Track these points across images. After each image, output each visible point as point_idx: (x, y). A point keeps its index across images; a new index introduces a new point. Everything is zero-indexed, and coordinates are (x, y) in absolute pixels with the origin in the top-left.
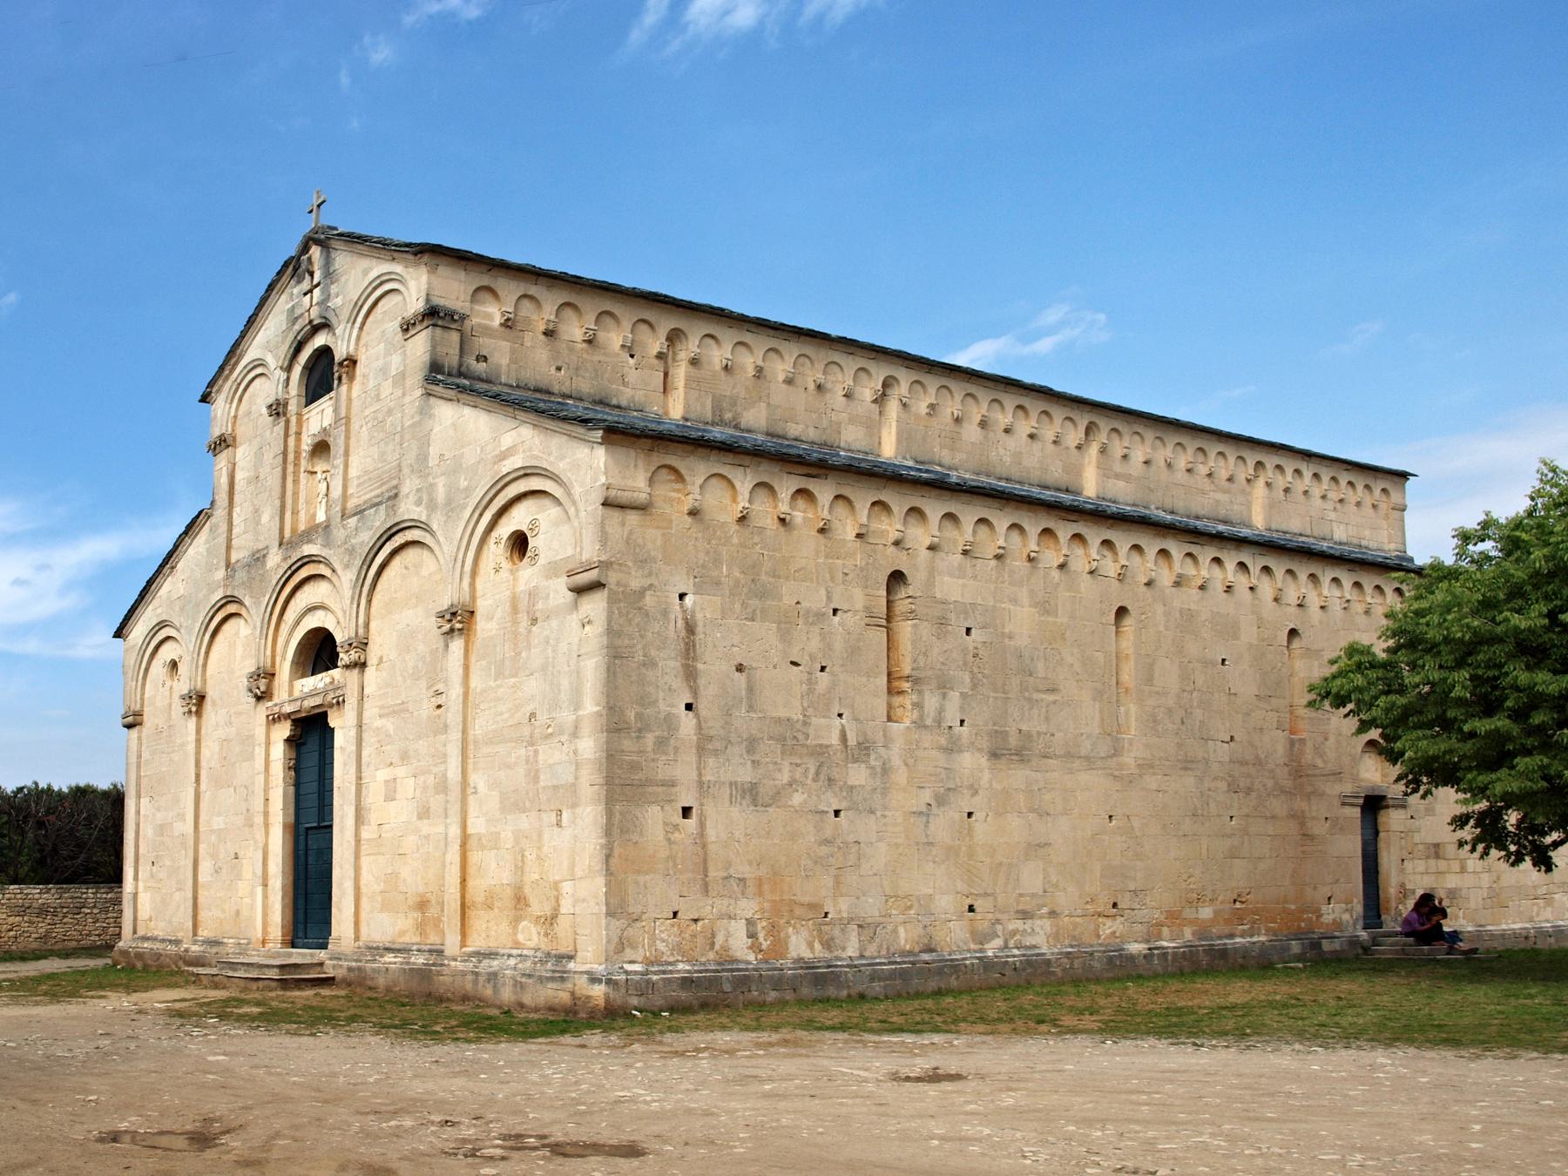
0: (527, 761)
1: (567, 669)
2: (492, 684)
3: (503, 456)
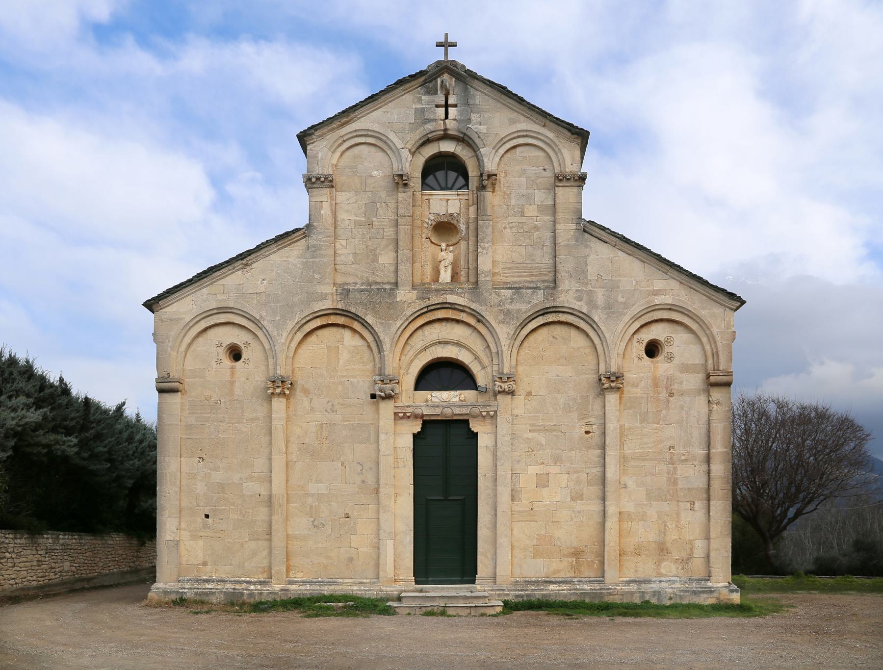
0: (668, 473)
1: (696, 425)
2: (638, 425)
3: (657, 293)
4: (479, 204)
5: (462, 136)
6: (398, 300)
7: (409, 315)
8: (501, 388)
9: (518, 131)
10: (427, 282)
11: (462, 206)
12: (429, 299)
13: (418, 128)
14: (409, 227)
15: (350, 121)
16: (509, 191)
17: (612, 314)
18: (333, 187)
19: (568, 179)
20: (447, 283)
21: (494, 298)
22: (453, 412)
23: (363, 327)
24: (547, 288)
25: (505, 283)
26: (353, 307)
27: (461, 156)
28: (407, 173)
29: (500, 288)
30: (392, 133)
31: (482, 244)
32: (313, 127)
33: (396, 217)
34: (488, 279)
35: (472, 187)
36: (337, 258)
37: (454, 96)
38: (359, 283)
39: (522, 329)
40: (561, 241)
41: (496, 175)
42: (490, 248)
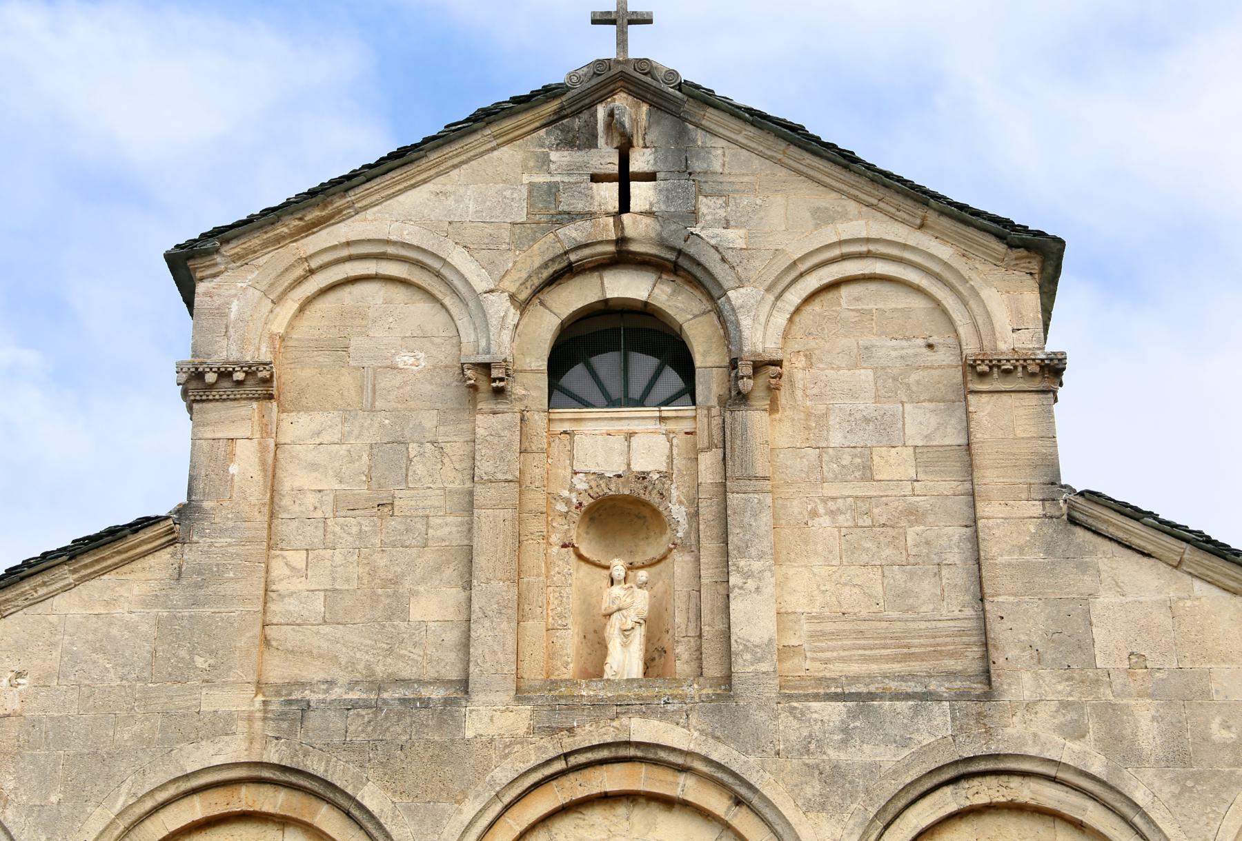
4: (728, 445)
5: (671, 256)
6: (469, 734)
7: (505, 782)
9: (841, 243)
10: (567, 677)
11: (675, 452)
12: (571, 730)
13: (538, 235)
14: (508, 514)
15: (331, 217)
16: (821, 408)
17: (1197, 782)
18: (270, 397)
19: (1007, 372)
20: (630, 681)
21: (788, 729)
23: (348, 822)
24: (962, 695)
25: (820, 681)
26: (316, 758)
27: (670, 313)
28: (505, 361)
29: (807, 697)
30: (459, 249)
31: (742, 563)
32: (217, 232)
33: (468, 485)
34: (764, 667)
35: (707, 398)
36: (273, 607)
37: (648, 151)
38: (341, 681)
39: (886, 827)
40: (998, 551)
41: (778, 363)
42: (768, 574)
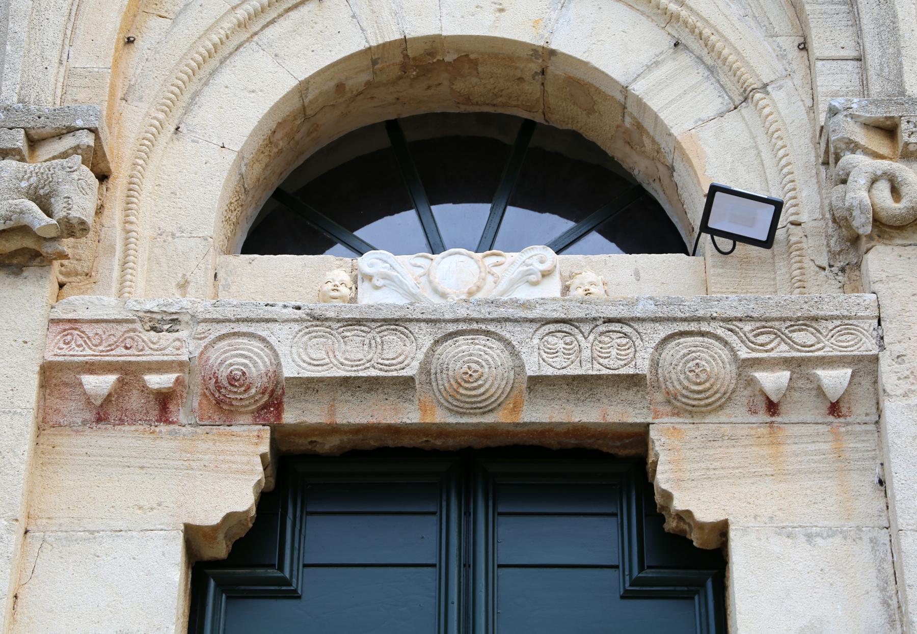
8: (895, 192)
22: (520, 367)
